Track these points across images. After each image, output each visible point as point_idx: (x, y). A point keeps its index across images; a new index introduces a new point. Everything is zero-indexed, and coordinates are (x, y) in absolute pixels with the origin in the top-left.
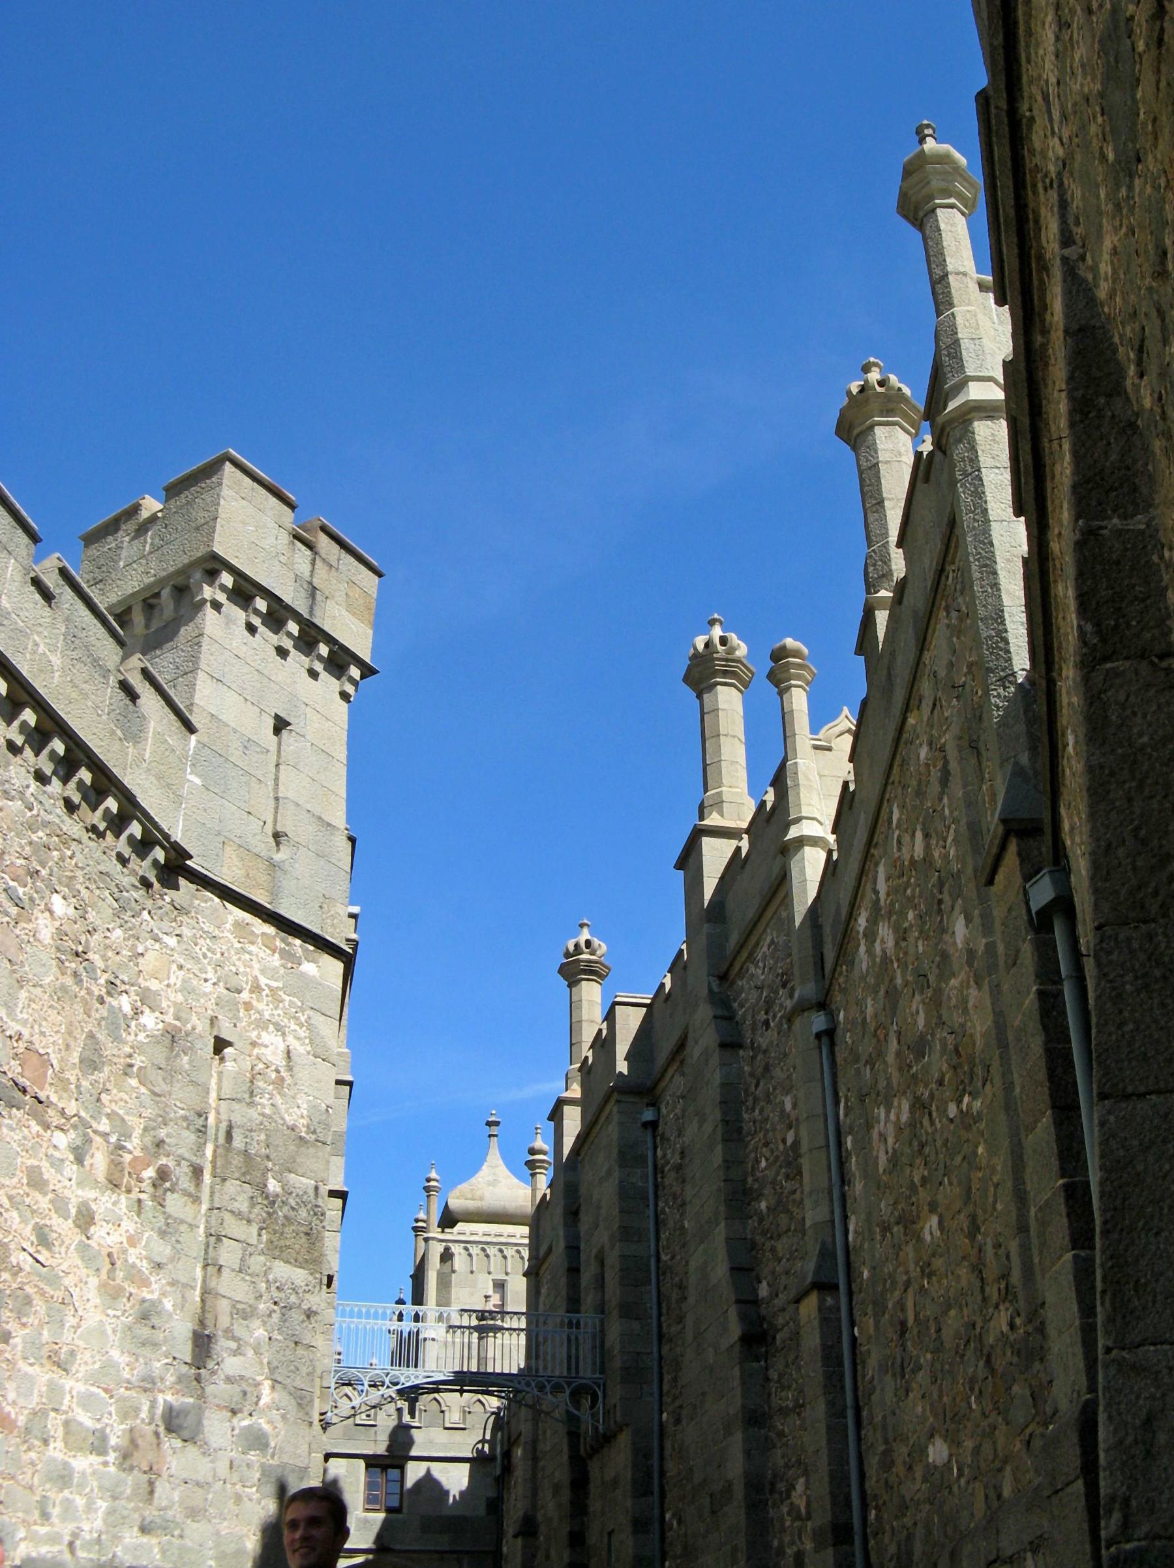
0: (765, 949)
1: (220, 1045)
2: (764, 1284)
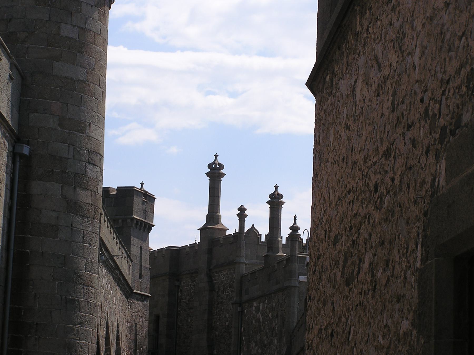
0: (225, 273)
1: (135, 324)
2: (215, 351)
